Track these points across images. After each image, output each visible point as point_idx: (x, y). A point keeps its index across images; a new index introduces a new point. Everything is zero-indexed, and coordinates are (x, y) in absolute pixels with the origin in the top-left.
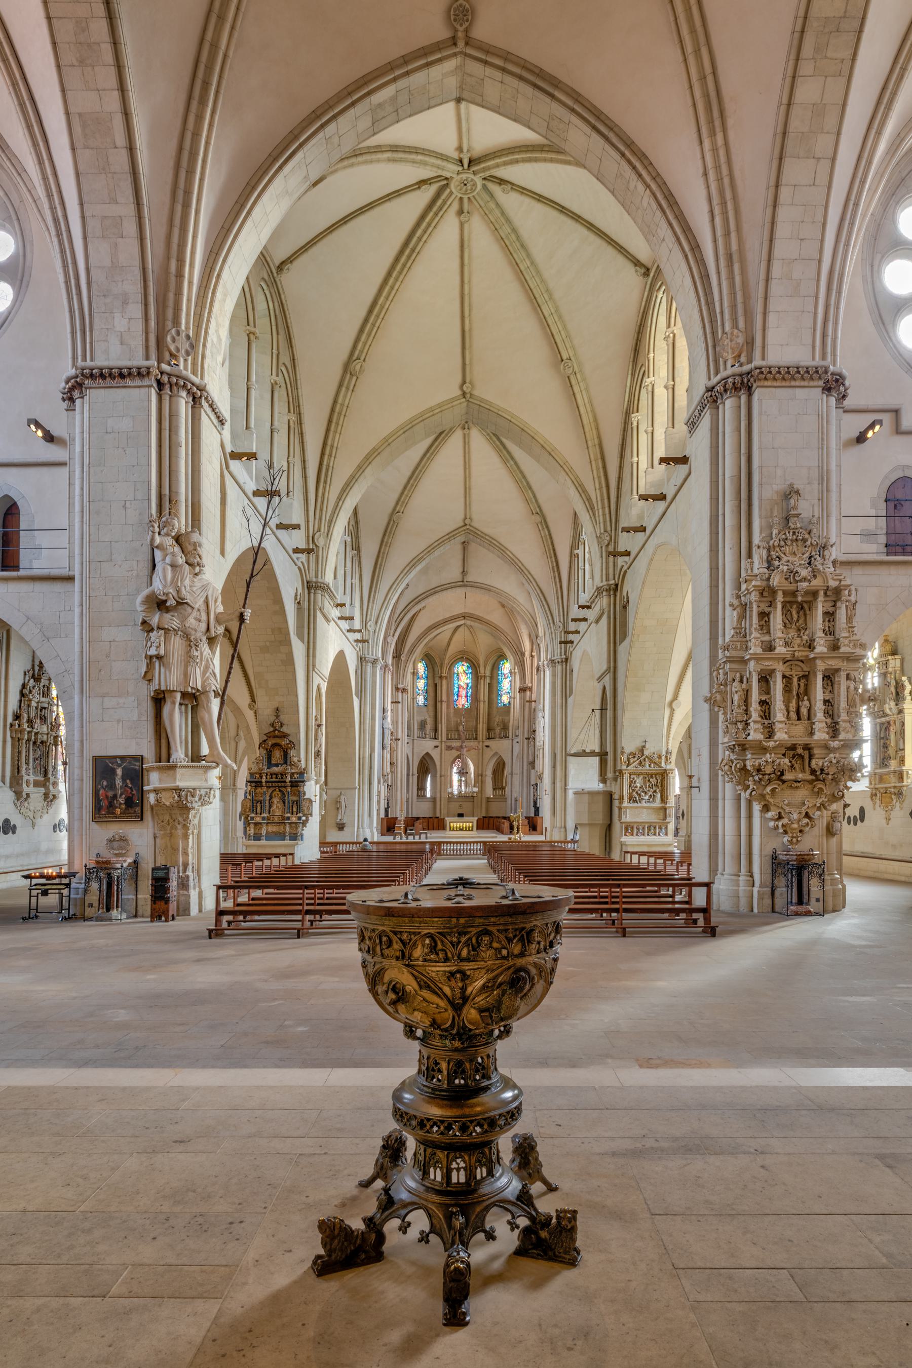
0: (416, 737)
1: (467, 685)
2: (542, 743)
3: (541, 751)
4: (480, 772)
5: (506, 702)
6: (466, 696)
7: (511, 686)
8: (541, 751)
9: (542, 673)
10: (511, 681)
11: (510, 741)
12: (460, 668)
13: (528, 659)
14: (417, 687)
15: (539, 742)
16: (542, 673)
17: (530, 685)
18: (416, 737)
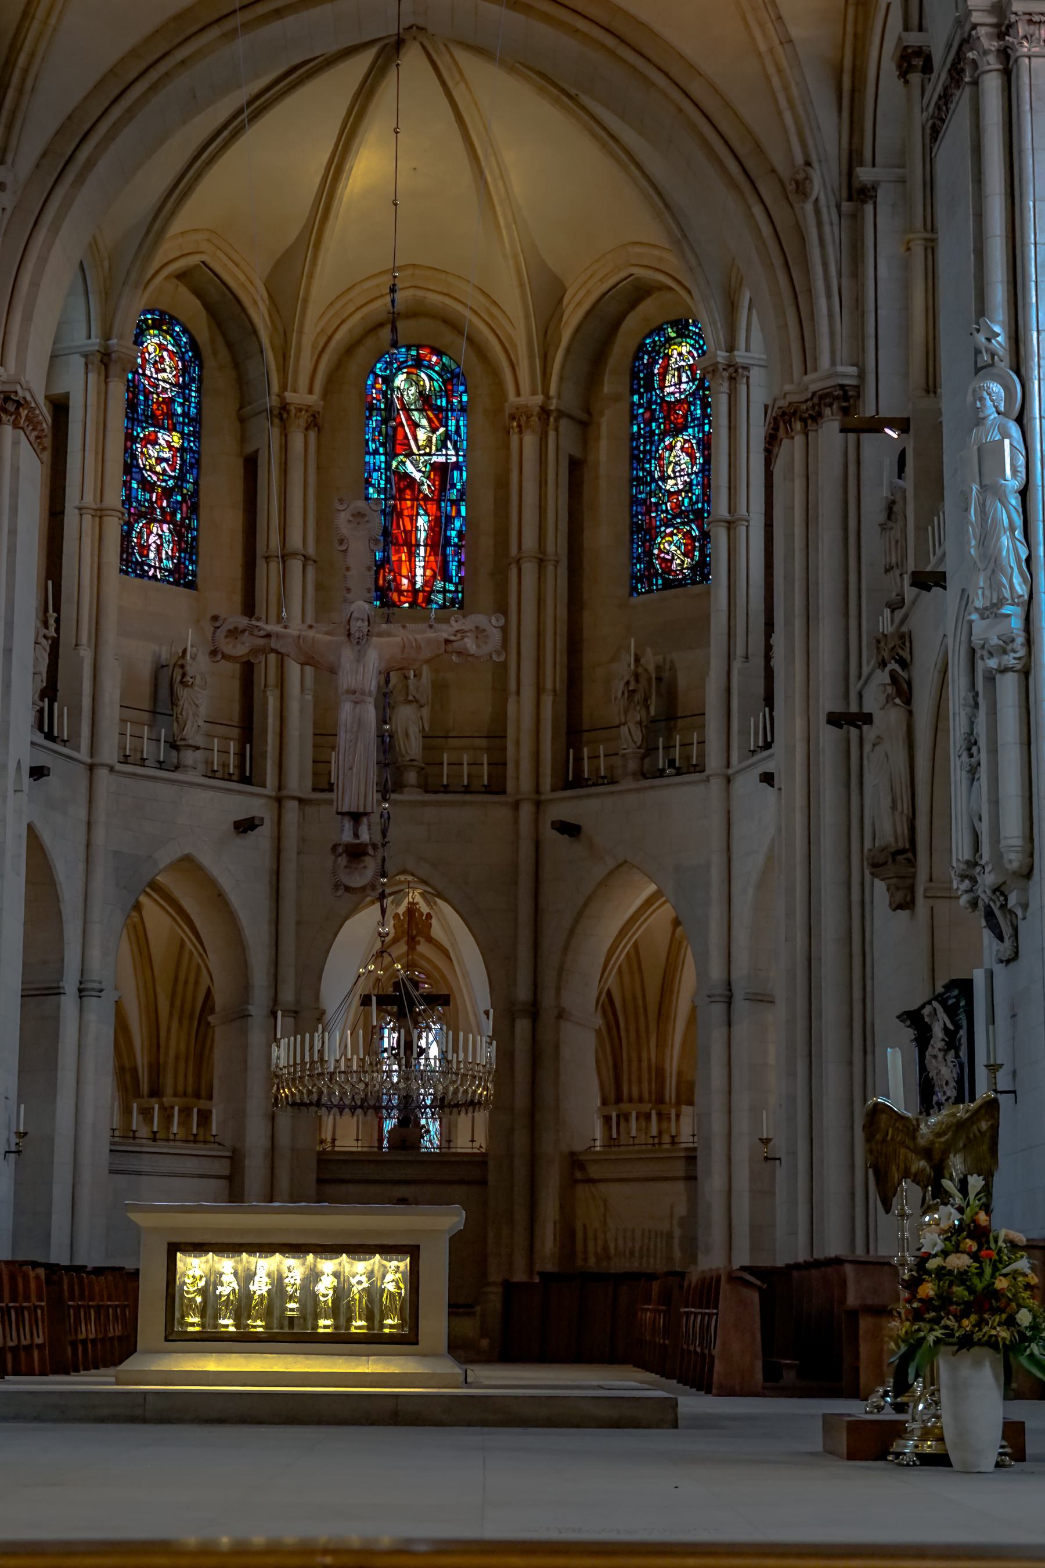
0: (109, 753)
1: (442, 471)
2: (1013, 612)
3: (1008, 687)
4: (523, 994)
5: (680, 563)
6: (437, 542)
7: (706, 469)
8: (1008, 687)
9: (992, 85)
10: (705, 444)
11: (716, 785)
12: (400, 381)
13: (828, 215)
14: (130, 467)
15: (992, 611)
16: (992, 85)
17: (847, 373)
18: (109, 753)
